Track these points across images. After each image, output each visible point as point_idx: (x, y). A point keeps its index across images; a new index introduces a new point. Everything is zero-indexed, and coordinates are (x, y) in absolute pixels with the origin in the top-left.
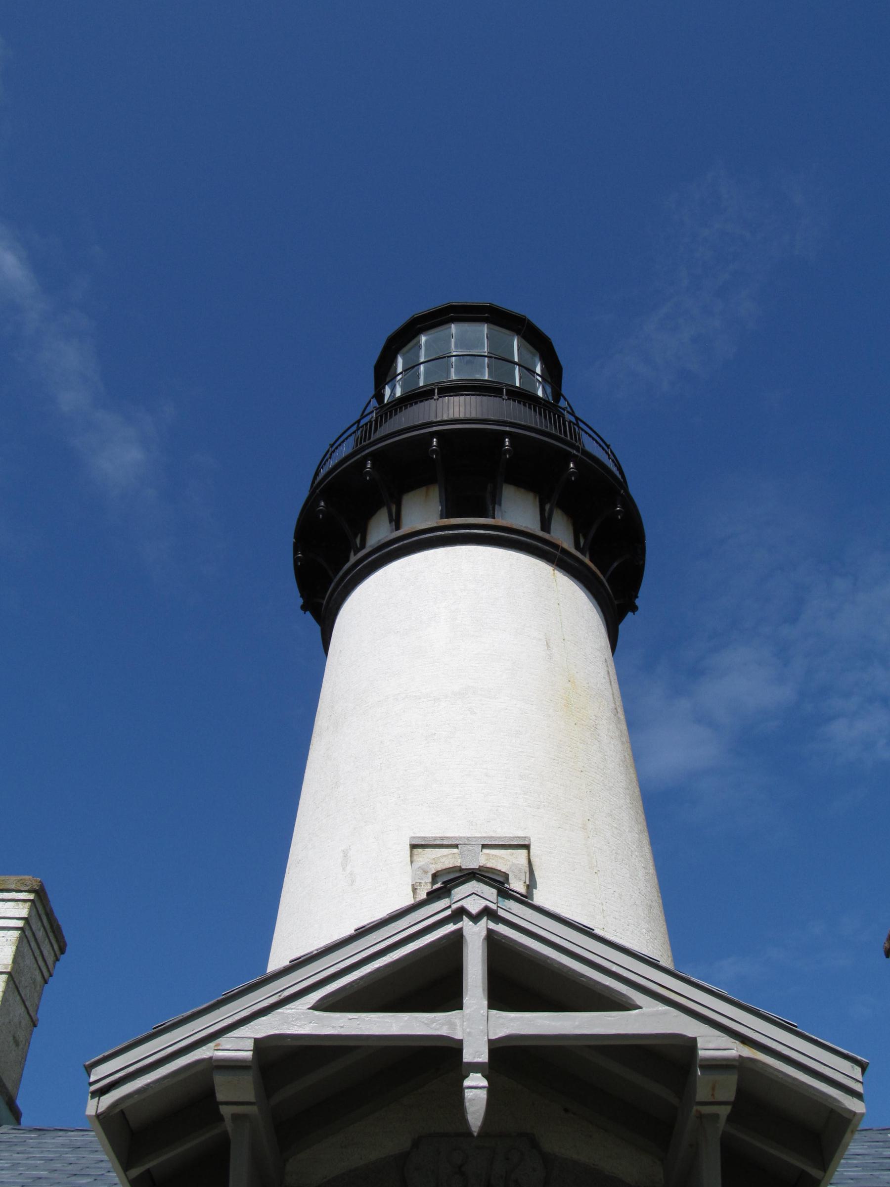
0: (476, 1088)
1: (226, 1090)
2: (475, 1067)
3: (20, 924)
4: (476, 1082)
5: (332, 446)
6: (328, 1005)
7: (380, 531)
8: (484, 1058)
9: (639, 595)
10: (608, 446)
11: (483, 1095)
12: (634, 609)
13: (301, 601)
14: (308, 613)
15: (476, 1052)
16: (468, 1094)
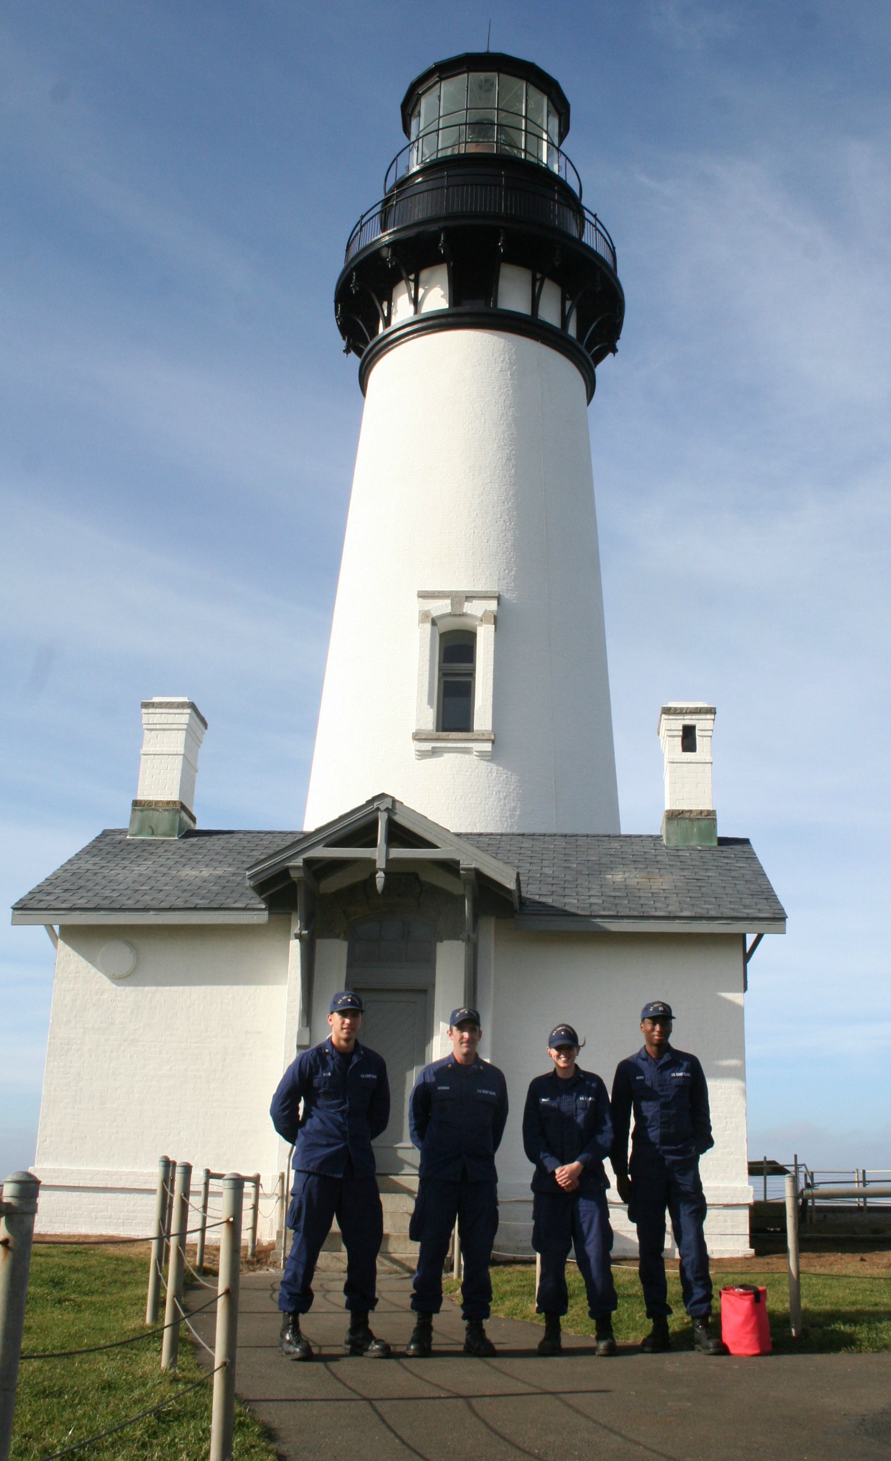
0: (380, 875)
1: (294, 874)
2: (381, 870)
3: (185, 727)
4: (380, 875)
5: (363, 217)
6: (328, 845)
7: (402, 310)
8: (383, 866)
9: (622, 336)
10: (595, 216)
11: (383, 880)
12: (614, 351)
13: (343, 344)
14: (352, 354)
15: (381, 864)
16: (378, 880)
